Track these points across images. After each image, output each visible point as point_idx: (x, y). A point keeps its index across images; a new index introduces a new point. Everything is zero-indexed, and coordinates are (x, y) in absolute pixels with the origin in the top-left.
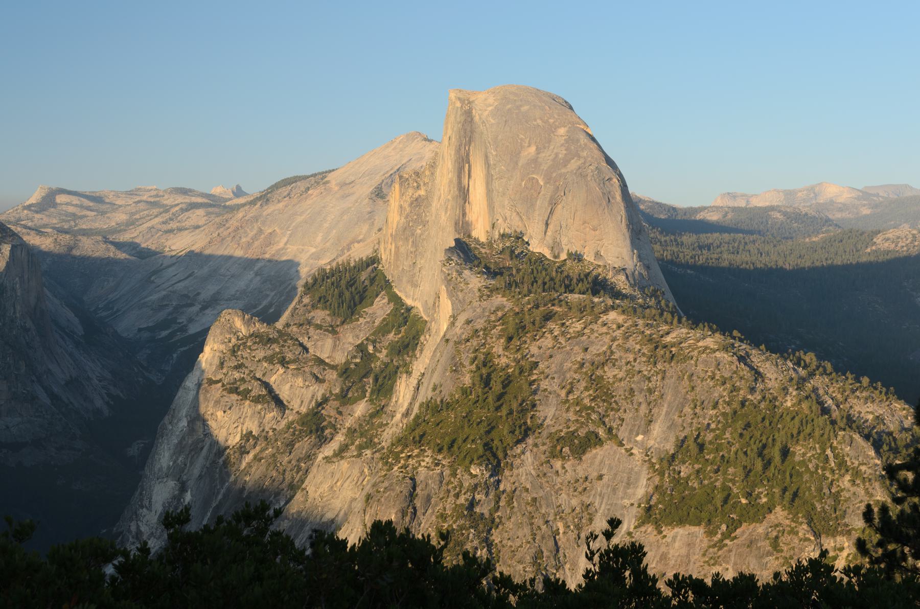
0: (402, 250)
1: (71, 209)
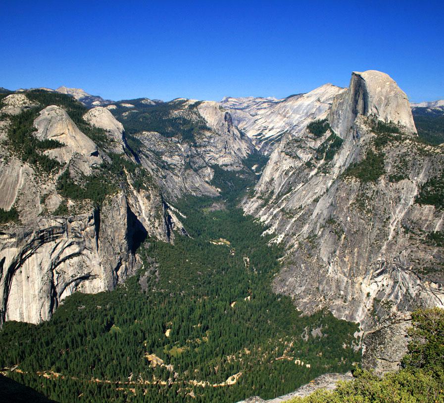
0: (335, 117)
1: (232, 102)
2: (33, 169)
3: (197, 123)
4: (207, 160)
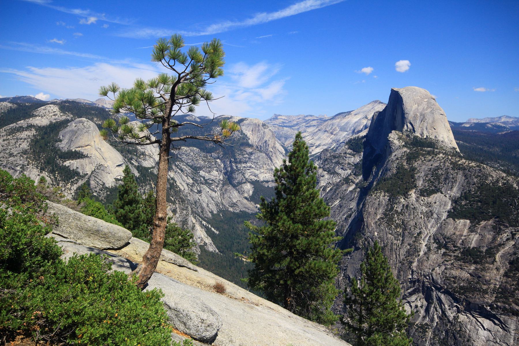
1: (282, 120)
2: (51, 178)
3: (239, 140)
4: (247, 176)
